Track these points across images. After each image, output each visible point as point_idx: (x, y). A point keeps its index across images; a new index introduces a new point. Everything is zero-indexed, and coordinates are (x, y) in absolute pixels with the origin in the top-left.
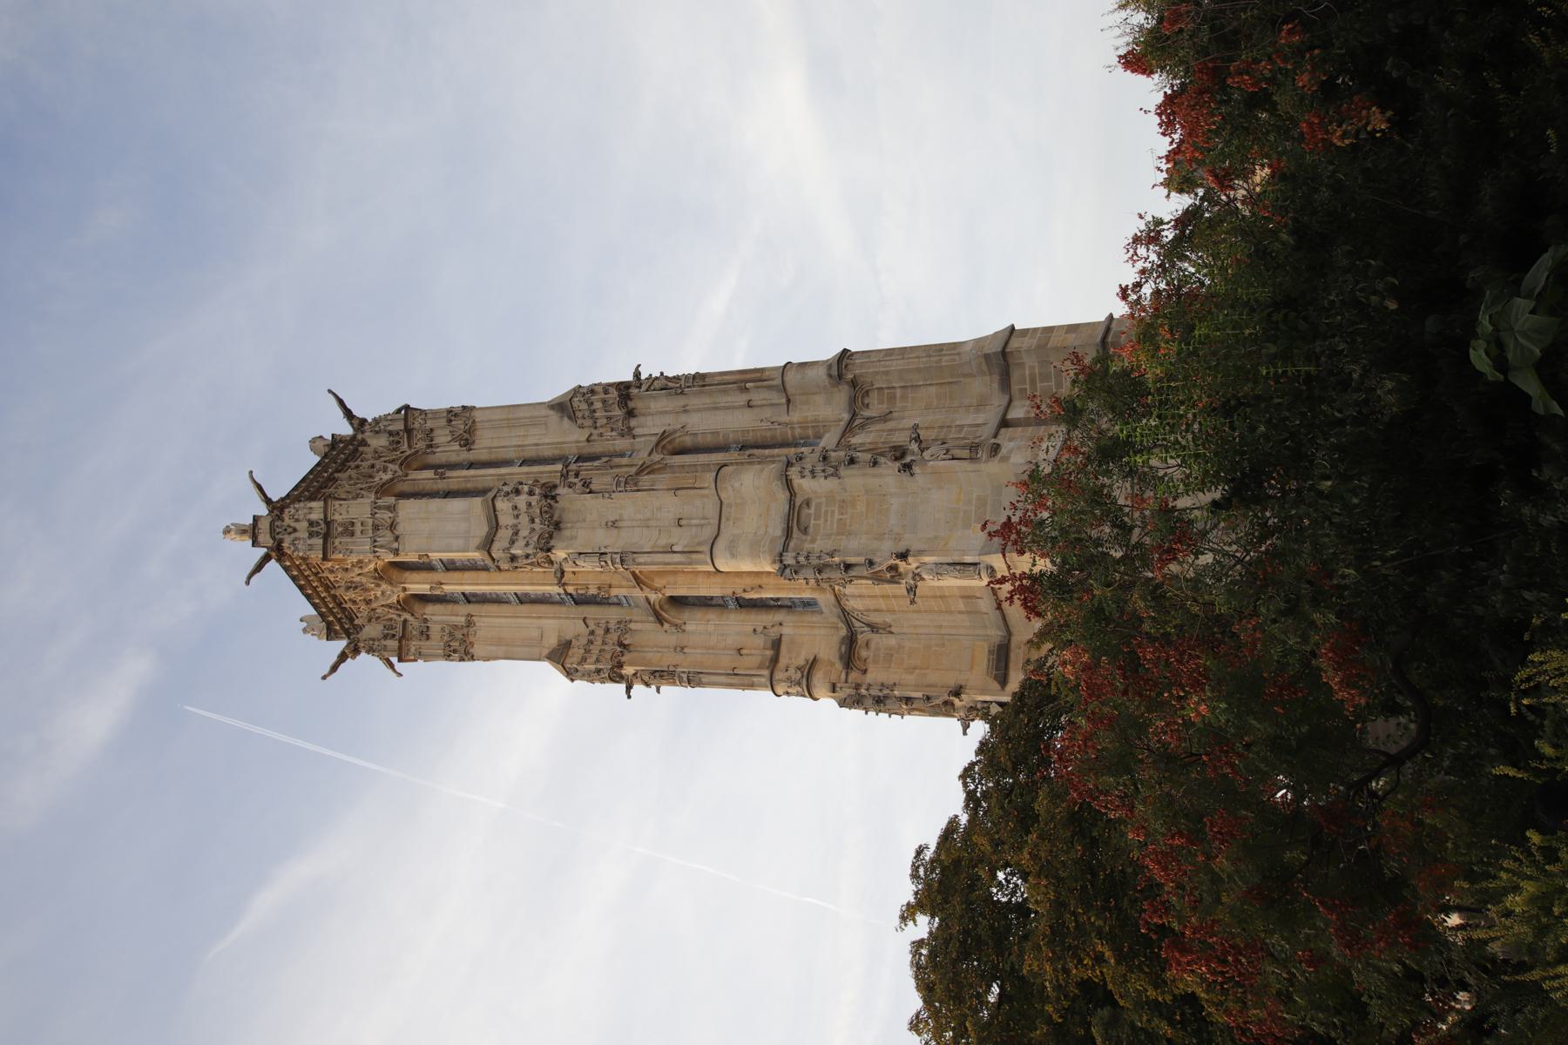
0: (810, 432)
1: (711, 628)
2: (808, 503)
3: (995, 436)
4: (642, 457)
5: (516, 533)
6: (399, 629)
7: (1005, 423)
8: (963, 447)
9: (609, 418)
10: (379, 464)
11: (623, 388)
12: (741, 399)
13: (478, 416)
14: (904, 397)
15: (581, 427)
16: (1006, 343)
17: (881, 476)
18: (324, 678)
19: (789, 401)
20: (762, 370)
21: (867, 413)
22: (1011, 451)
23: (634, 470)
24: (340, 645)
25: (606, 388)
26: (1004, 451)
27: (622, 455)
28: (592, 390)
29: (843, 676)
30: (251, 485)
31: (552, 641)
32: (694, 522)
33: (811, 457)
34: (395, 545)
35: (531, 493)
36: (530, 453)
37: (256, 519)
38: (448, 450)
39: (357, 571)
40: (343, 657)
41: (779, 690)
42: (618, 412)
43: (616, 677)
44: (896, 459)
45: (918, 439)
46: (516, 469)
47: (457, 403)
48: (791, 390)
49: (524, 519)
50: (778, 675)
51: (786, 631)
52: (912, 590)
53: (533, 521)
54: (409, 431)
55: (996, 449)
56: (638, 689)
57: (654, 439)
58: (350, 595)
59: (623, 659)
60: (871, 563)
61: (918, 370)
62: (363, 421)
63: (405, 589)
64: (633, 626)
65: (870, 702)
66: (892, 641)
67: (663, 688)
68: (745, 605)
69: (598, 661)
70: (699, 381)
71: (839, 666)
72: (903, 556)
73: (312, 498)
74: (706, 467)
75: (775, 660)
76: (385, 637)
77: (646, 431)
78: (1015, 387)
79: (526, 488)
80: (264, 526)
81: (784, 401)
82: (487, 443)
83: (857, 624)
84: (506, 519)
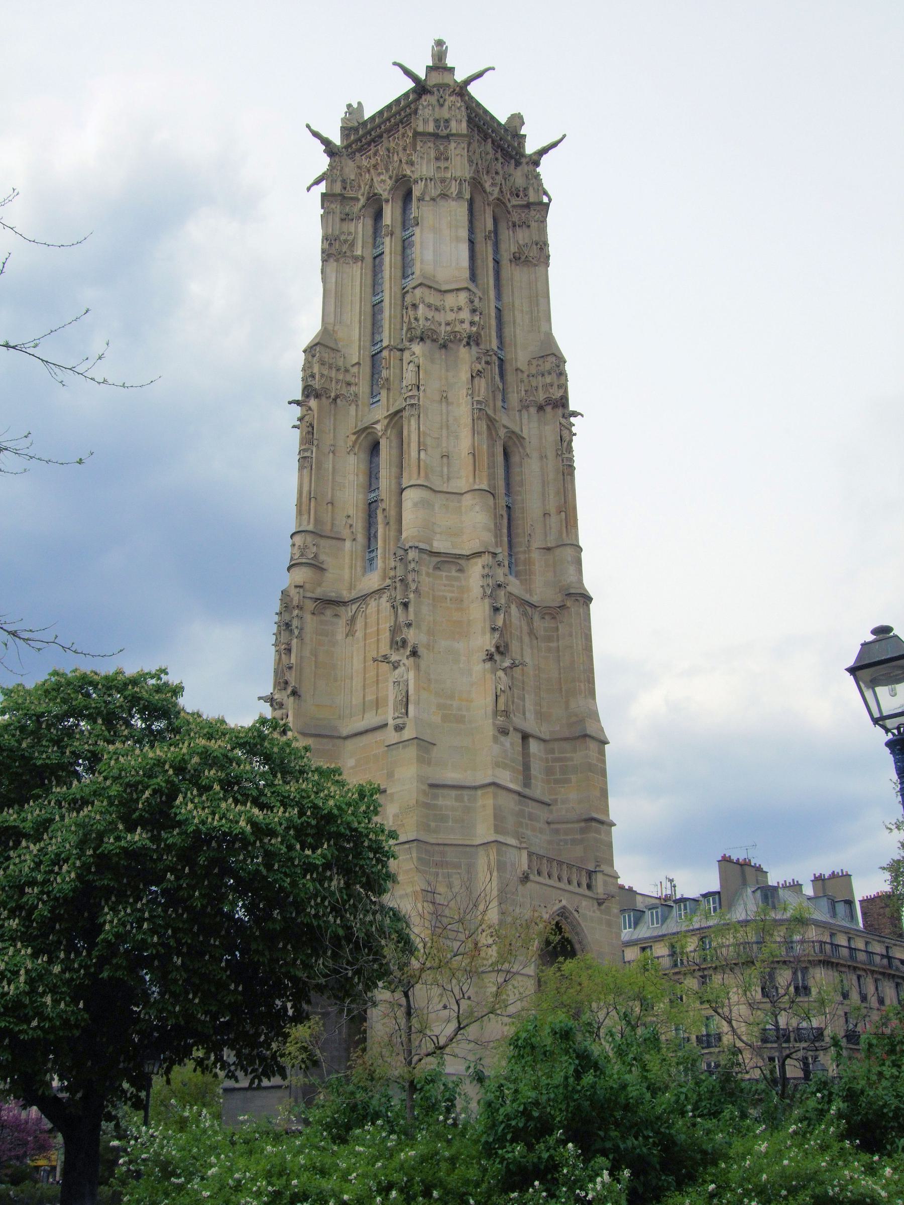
0: (521, 568)
2: (461, 570)
3: (515, 729)
5: (437, 309)
6: (351, 194)
7: (525, 737)
8: (507, 705)
10: (499, 179)
11: (562, 402)
12: (552, 508)
13: (540, 269)
17: (484, 633)
18: (308, 126)
19: (549, 549)
21: (536, 617)
22: (502, 745)
23: (490, 412)
24: (336, 139)
26: (502, 739)
27: (503, 401)
28: (562, 374)
29: (309, 595)
30: (482, 68)
32: (445, 470)
33: (500, 574)
34: (427, 198)
35: (472, 323)
36: (507, 317)
37: (452, 70)
41: (298, 539)
42: (541, 397)
43: (308, 391)
44: (497, 648)
45: (514, 666)
46: (493, 305)
47: (552, 250)
48: (558, 551)
49: (451, 316)
50: (309, 539)
51: (348, 544)
53: (448, 324)
55: (504, 732)
56: (297, 411)
59: (324, 399)
60: (409, 625)
62: (537, 164)
64: (353, 407)
65: (287, 617)
67: (298, 431)
68: (371, 508)
69: (322, 375)
70: (568, 470)
73: (470, 120)
74: (492, 477)
76: (344, 181)
77: (525, 421)
79: (477, 319)
80: (446, 79)
81: (549, 545)
82: (515, 276)
83: (354, 607)
84: (450, 300)
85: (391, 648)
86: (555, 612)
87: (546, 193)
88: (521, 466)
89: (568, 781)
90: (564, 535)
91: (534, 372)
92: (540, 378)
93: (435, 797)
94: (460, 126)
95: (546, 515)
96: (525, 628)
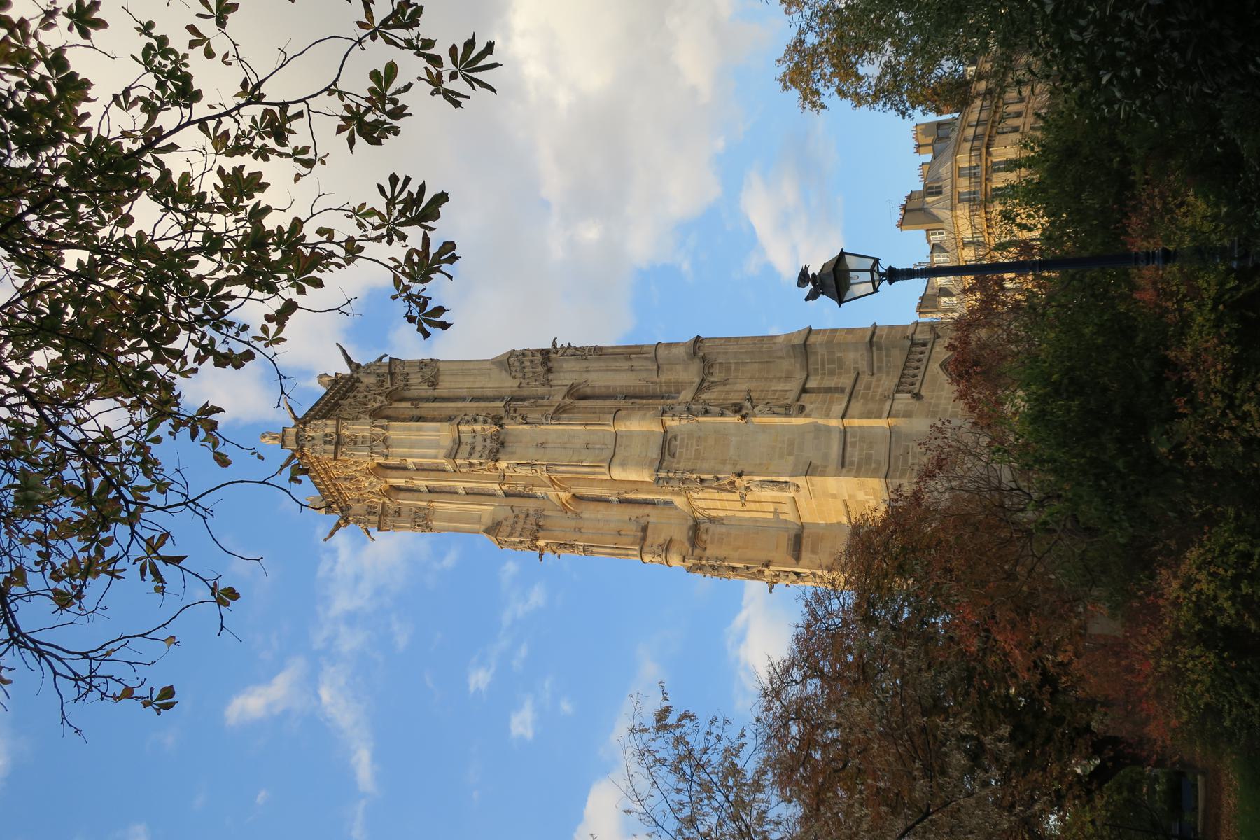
1: (600, 516)
4: (557, 399)
6: (379, 508)
7: (804, 390)
8: (781, 406)
10: (370, 396)
11: (545, 353)
12: (627, 365)
14: (737, 370)
15: (515, 378)
16: (807, 339)
20: (641, 347)
21: (712, 379)
23: (553, 409)
24: (336, 517)
26: (807, 410)
27: (543, 398)
28: (523, 354)
31: (487, 521)
35: (485, 422)
36: (478, 393)
38: (418, 387)
40: (338, 526)
42: (541, 369)
45: (750, 400)
46: (467, 404)
48: (660, 361)
49: (479, 439)
50: (646, 549)
51: (651, 520)
52: (743, 498)
54: (391, 374)
57: (565, 389)
58: (348, 484)
61: (746, 352)
62: (358, 366)
66: (723, 529)
69: (521, 535)
71: (687, 544)
72: (740, 475)
74: (603, 411)
75: (644, 539)
76: (369, 513)
77: (560, 383)
78: (811, 367)
82: (447, 385)
84: (465, 438)
86: (707, 365)
87: (380, 359)
89: (840, 359)
93: (852, 463)
94: (329, 426)
96: (720, 388)
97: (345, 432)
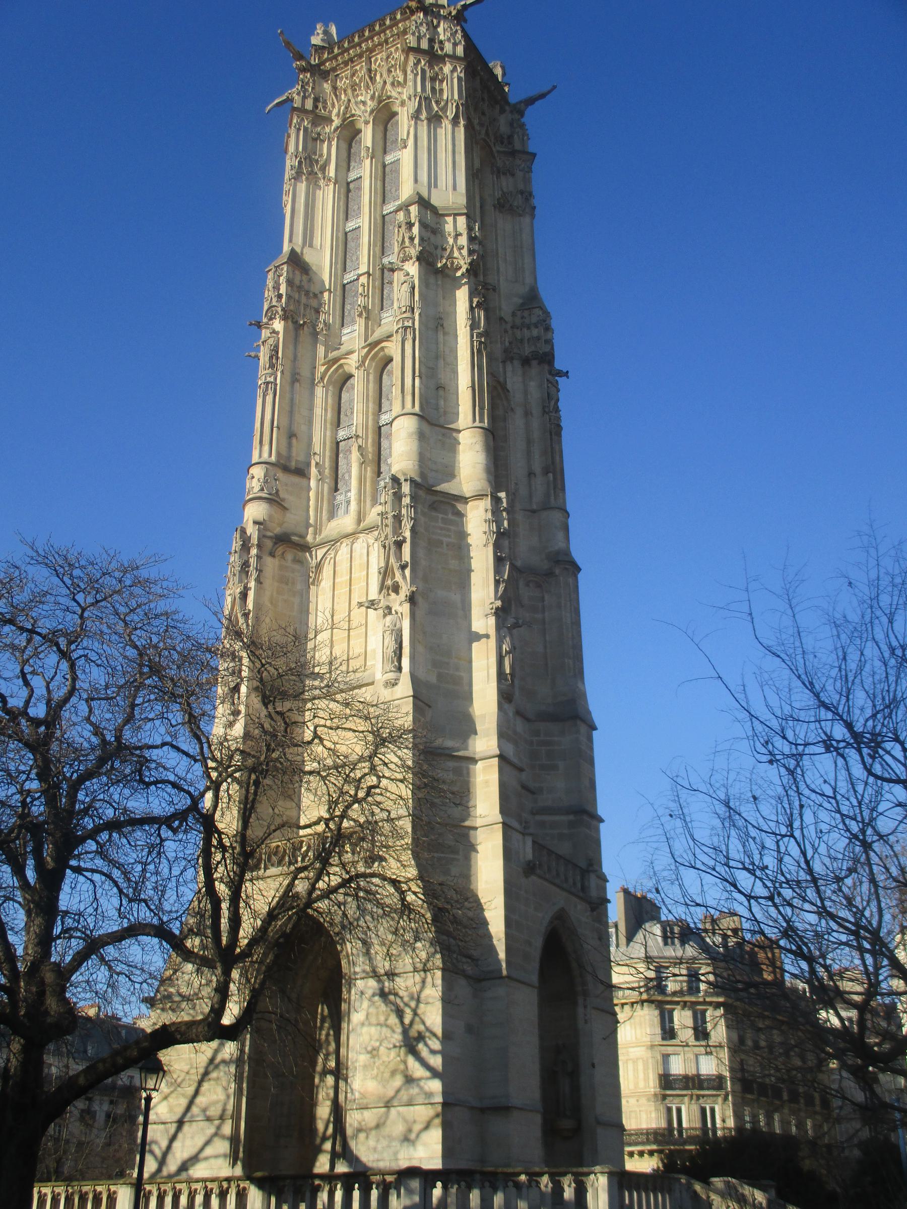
9: (522, 341)
11: (547, 359)
12: (537, 467)
13: (527, 219)
15: (514, 314)
19: (534, 511)
21: (521, 584)
25: (549, 342)
28: (548, 329)
29: (269, 534)
39: (389, 81)
42: (527, 350)
52: (372, 604)
54: (513, 153)
57: (501, 380)
62: (522, 114)
63: (367, 123)
71: (278, 530)
75: (286, 469)
77: (509, 374)
81: (535, 507)
85: (380, 592)
88: (505, 420)
90: (552, 498)
91: (518, 321)
92: (525, 330)
95: (531, 474)
97: (447, 68)
